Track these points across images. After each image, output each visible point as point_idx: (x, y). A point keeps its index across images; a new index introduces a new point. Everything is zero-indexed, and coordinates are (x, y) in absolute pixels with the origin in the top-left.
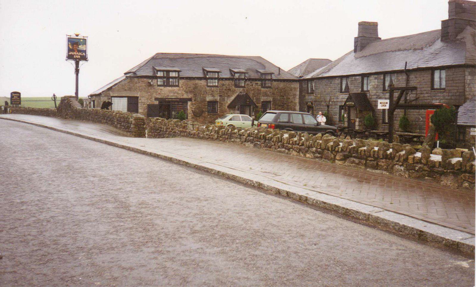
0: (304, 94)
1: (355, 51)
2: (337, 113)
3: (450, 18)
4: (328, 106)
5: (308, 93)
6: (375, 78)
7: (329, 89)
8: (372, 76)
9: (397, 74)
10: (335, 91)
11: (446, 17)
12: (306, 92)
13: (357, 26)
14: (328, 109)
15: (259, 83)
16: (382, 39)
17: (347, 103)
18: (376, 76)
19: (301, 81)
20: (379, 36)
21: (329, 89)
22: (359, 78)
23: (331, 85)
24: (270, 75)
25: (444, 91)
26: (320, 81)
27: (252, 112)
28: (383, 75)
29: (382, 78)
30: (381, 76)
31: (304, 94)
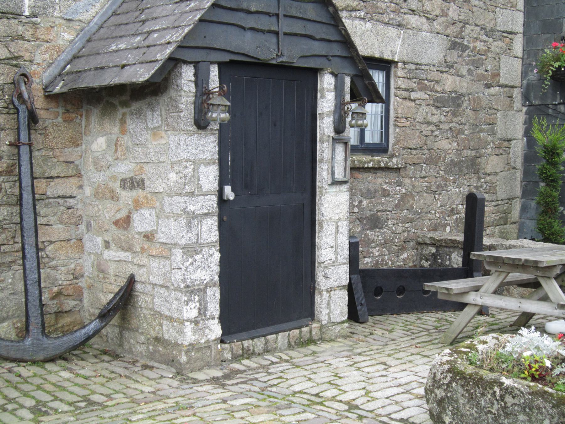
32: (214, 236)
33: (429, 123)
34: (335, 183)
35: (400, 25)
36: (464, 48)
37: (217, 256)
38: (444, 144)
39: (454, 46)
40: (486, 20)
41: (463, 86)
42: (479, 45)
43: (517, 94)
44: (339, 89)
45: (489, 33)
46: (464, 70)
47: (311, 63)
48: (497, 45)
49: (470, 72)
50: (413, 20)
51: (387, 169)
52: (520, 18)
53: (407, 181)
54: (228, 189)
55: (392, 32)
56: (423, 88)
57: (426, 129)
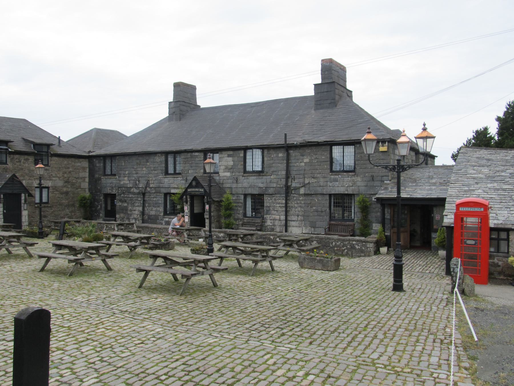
0: (97, 176)
1: (169, 119)
2: (160, 204)
3: (324, 82)
4: (144, 194)
5: (105, 175)
6: (229, 156)
7: (144, 169)
8: (224, 153)
9: (268, 151)
10: (156, 172)
11: (319, 81)
12: (101, 172)
13: (172, 88)
14: (144, 197)
15: (31, 159)
16: (201, 107)
17: (189, 190)
18: (231, 153)
19: (90, 158)
20: (198, 104)
21: (144, 169)
22: (202, 155)
23: (148, 164)
24: (46, 147)
25: (353, 174)
26: (127, 158)
27: (24, 204)
28: (243, 152)
29: (242, 155)
30: (239, 152)
31: (97, 176)
32: (2, 217)
33: (59, 198)
34: (24, 210)
35: (51, 180)
36: (69, 182)
37: (3, 220)
38: (64, 201)
39: (66, 182)
40: (77, 176)
41: (69, 190)
42: (74, 181)
43: (87, 190)
44: (25, 196)
45: (78, 178)
46: (69, 186)
47: (19, 193)
48: (79, 181)
49: (71, 187)
50: (54, 179)
51: (47, 207)
52: (87, 175)
53: (53, 209)
54: (5, 211)
55: (48, 181)
56: (57, 191)
57: (58, 199)
